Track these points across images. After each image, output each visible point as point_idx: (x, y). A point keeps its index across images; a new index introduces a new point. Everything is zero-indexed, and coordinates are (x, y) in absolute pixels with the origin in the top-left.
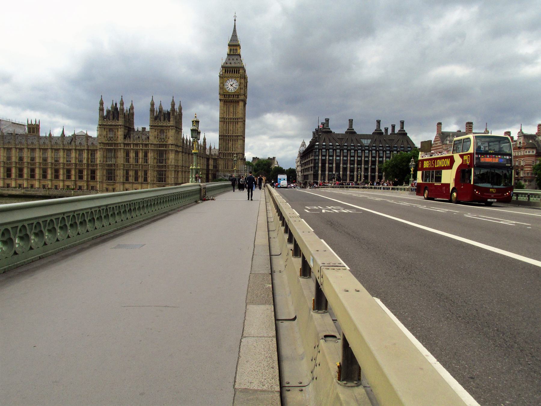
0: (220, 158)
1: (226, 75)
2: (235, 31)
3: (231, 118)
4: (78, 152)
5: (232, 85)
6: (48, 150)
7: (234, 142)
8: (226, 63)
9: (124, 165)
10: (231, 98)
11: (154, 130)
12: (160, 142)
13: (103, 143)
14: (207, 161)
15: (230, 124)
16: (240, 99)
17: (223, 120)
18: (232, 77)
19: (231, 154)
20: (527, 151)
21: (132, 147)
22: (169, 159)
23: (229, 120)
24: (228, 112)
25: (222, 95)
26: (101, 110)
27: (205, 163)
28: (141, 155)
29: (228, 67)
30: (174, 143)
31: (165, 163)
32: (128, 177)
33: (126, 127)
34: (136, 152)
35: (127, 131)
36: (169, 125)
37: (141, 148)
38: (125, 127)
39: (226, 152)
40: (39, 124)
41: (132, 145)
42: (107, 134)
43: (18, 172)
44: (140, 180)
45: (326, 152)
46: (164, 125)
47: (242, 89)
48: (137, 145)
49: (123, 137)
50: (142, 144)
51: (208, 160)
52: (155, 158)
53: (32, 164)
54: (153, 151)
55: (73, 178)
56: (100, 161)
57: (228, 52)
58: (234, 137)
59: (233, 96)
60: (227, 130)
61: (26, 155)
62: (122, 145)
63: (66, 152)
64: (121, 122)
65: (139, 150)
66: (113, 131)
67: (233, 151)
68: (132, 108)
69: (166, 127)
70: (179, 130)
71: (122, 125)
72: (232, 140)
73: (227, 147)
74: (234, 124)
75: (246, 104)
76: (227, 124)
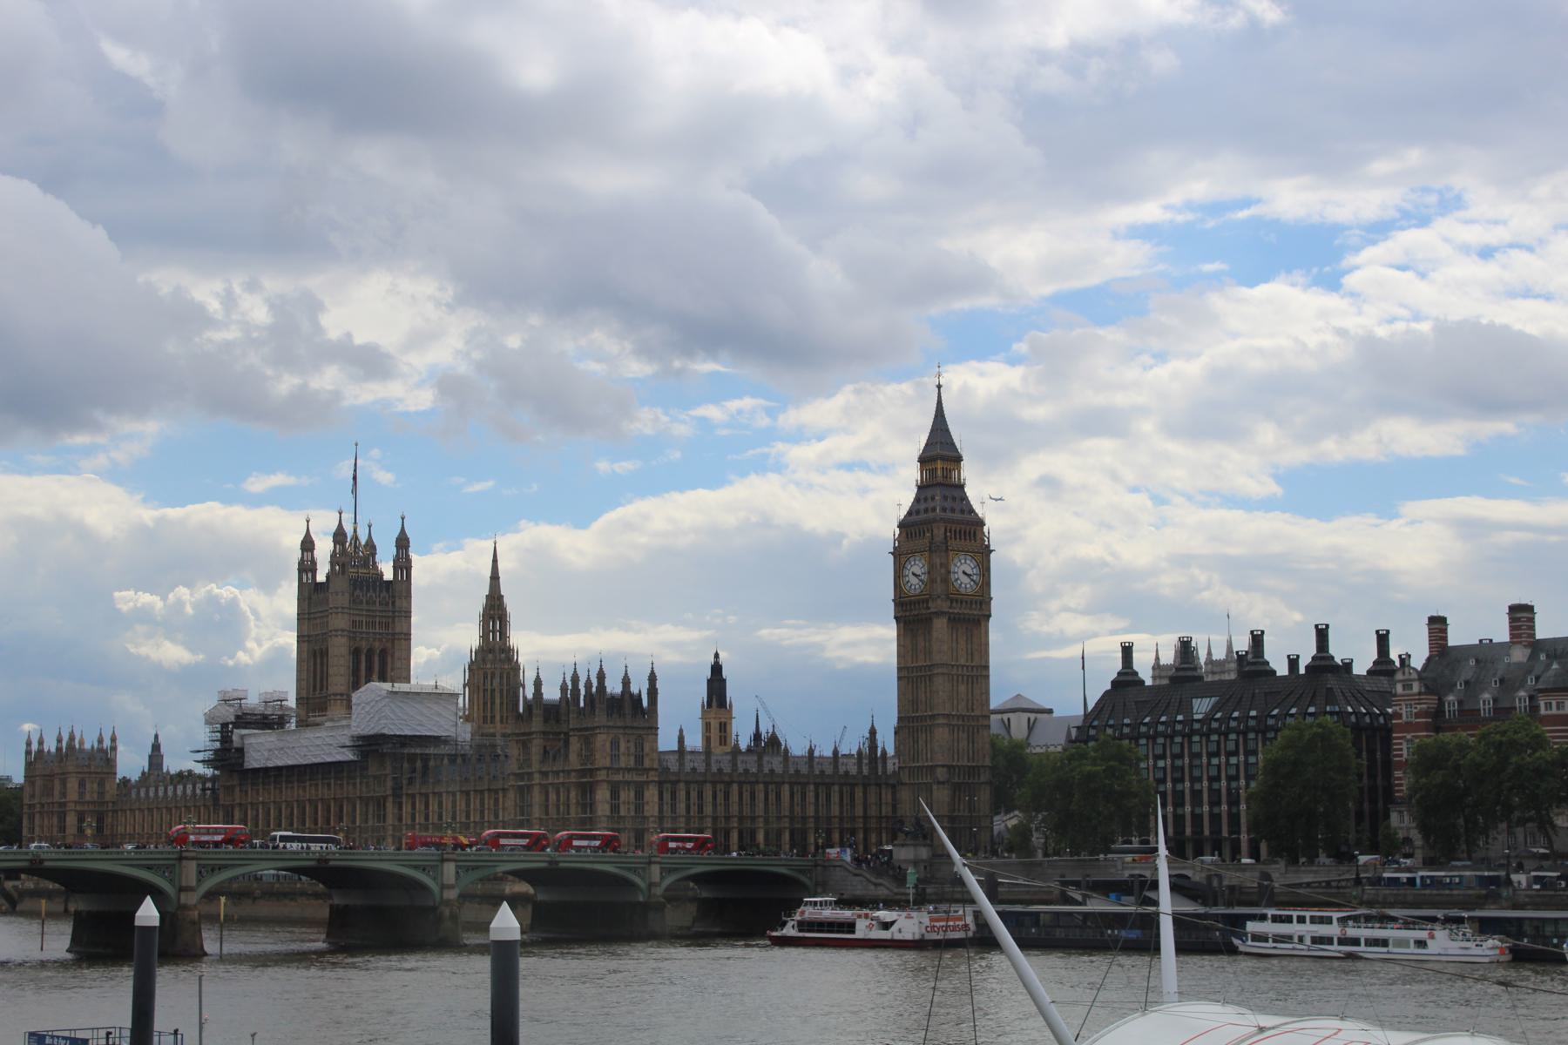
3: (921, 667)
7: (929, 735)
10: (915, 609)
12: (582, 765)
13: (515, 774)
16: (935, 610)
18: (913, 552)
19: (924, 770)
20: (1554, 703)
23: (917, 672)
27: (872, 799)
31: (591, 813)
37: (561, 780)
39: (914, 765)
41: (551, 774)
46: (589, 726)
47: (936, 582)
48: (557, 773)
50: (563, 771)
52: (578, 803)
57: (919, 479)
58: (928, 720)
62: (537, 776)
67: (927, 761)
70: (641, 732)
71: (537, 732)
72: (924, 728)
74: (928, 682)
75: (989, 616)
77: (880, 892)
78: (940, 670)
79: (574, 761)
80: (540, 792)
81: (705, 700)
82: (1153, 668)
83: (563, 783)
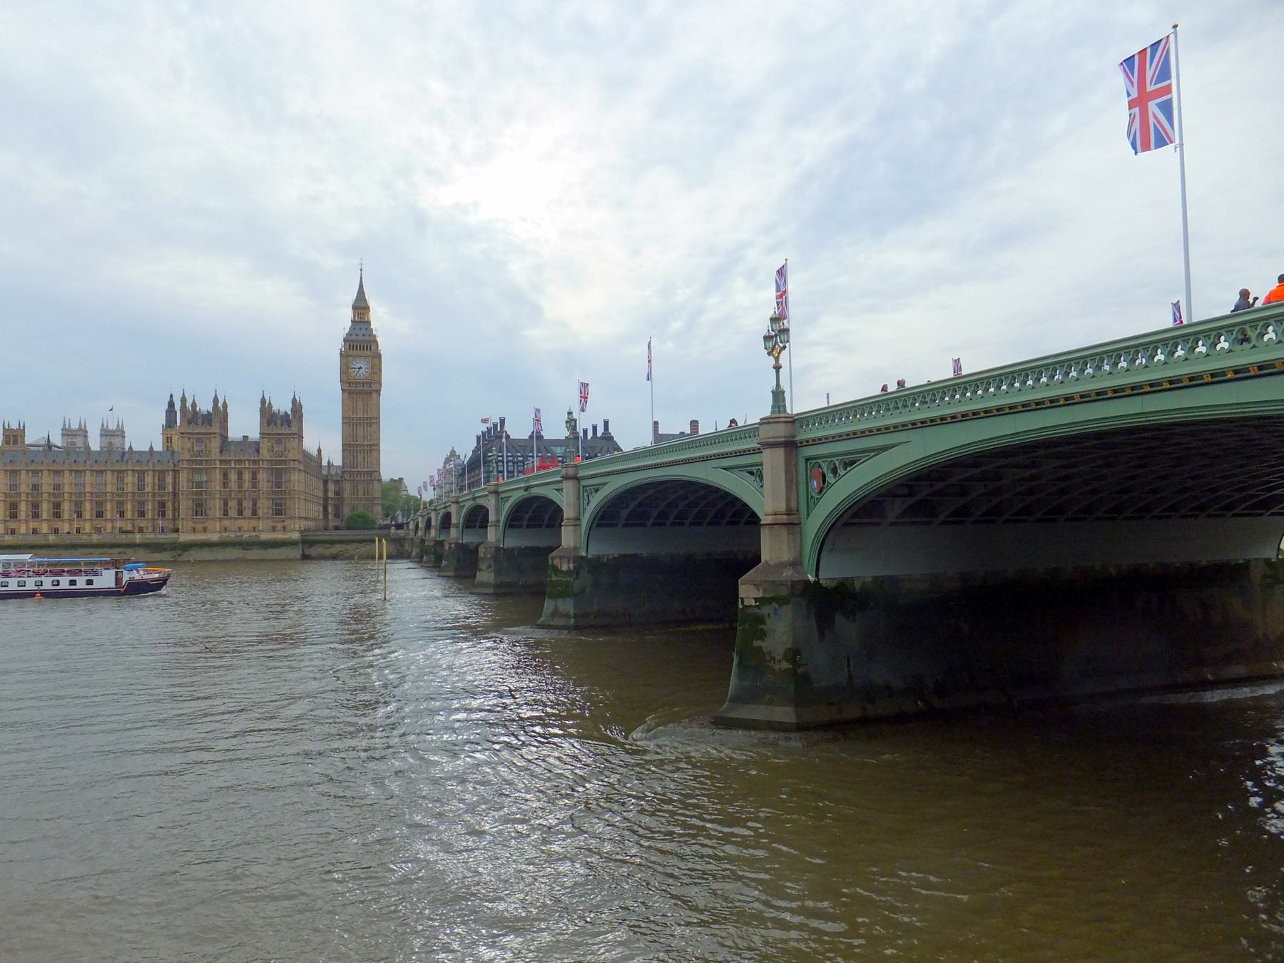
0: (345, 479)
1: (351, 352)
2: (361, 286)
4: (137, 475)
5: (361, 368)
6: (20, 474)
7: (366, 454)
8: (351, 335)
9: (221, 492)
13: (187, 460)
14: (324, 485)
17: (347, 422)
21: (233, 466)
22: (290, 481)
24: (355, 409)
25: (347, 382)
27: (322, 488)
28: (247, 476)
29: (352, 341)
30: (296, 459)
31: (285, 487)
32: (227, 510)
34: (238, 472)
36: (289, 432)
37: (247, 466)
38: (221, 435)
42: (193, 447)
43: (31, 509)
44: (247, 513)
48: (240, 462)
49: (218, 450)
50: (248, 460)
51: (326, 482)
53: (55, 496)
55: (129, 515)
56: (183, 487)
58: (366, 447)
59: (363, 384)
61: (46, 481)
62: (218, 462)
63: (116, 474)
64: (216, 428)
65: (243, 470)
66: (203, 442)
68: (225, 405)
69: (285, 435)
74: (365, 426)
76: (355, 428)
78: (375, 421)
79: (265, 454)
80: (220, 473)
81: (164, 423)
82: (62, 430)
83: (248, 468)
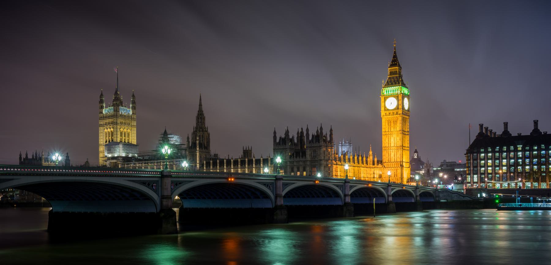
11: (309, 150)
15: (391, 138)
21: (295, 164)
26: (275, 137)
33: (292, 149)
35: (293, 152)
37: (301, 164)
38: (290, 148)
40: (251, 149)
45: (477, 155)
46: (315, 145)
50: (301, 161)
54: (309, 166)
60: (389, 143)
73: (390, 158)
76: (389, 138)
77: (466, 199)
79: (308, 157)
